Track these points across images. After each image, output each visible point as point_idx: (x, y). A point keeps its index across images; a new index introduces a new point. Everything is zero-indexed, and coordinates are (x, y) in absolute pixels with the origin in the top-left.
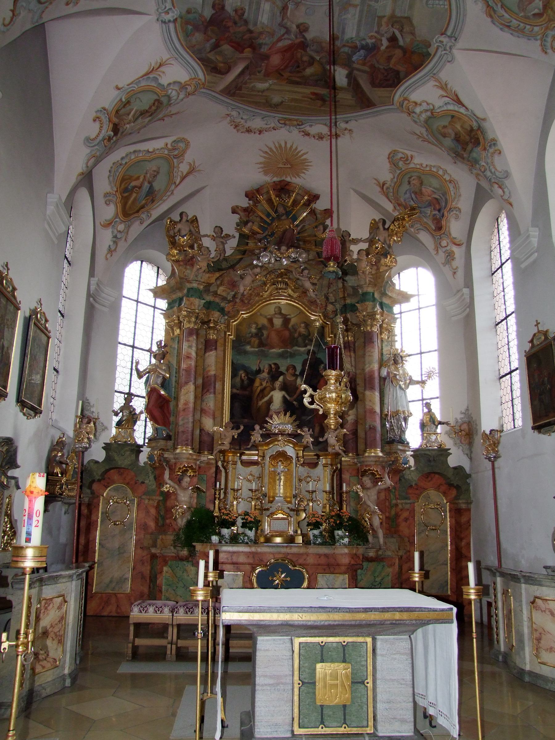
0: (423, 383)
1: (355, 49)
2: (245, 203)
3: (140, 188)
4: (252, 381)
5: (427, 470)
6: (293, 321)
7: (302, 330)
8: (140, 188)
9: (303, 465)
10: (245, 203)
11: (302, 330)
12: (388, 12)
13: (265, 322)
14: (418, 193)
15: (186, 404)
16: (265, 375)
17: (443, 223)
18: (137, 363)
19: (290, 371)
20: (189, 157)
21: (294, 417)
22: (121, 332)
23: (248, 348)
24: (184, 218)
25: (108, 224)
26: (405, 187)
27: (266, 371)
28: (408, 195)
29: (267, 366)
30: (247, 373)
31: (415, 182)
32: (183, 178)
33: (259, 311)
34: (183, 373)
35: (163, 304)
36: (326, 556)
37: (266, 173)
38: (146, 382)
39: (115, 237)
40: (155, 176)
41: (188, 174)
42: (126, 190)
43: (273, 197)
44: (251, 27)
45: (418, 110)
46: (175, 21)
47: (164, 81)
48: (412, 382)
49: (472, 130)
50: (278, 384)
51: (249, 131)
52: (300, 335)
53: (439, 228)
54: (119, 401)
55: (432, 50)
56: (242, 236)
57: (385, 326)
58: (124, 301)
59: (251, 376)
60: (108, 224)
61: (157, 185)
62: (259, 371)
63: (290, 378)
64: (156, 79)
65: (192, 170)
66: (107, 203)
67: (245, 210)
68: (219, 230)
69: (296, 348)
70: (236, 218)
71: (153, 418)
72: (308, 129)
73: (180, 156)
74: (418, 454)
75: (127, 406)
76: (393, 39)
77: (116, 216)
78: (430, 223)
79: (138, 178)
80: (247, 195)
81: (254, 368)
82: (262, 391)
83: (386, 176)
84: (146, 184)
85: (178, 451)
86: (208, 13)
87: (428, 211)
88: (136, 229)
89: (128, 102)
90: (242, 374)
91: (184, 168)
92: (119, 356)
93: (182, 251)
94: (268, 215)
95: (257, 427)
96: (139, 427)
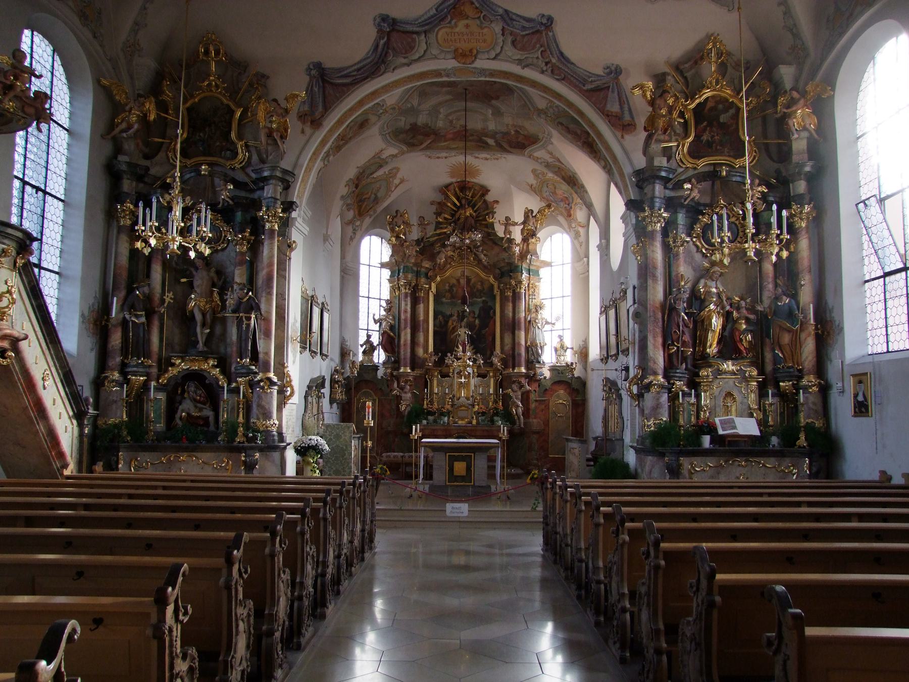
0: (554, 324)
1: (496, 133)
2: (440, 198)
3: (369, 198)
4: (447, 322)
5: (557, 379)
6: (473, 281)
7: (479, 287)
8: (369, 198)
9: (478, 377)
10: (440, 198)
11: (479, 287)
12: (511, 123)
13: (454, 281)
14: (554, 193)
15: (406, 341)
16: (455, 318)
17: (572, 212)
18: (374, 315)
19: (472, 315)
20: (399, 176)
21: (472, 347)
22: (361, 289)
23: (444, 300)
24: (399, 215)
25: (351, 222)
26: (545, 189)
27: (456, 315)
28: (548, 193)
29: (456, 312)
30: (443, 317)
31: (551, 186)
32: (396, 187)
33: (450, 274)
34: (402, 321)
35: (386, 273)
36: (487, 431)
37: (452, 177)
38: (380, 326)
39: (354, 230)
40: (378, 191)
41: (400, 183)
42: (360, 201)
43: (458, 192)
44: (433, 128)
45: (539, 161)
46: (389, 133)
47: (384, 156)
48: (547, 323)
49: (570, 177)
50: (463, 324)
51: (438, 158)
52: (478, 290)
53: (570, 215)
54: (362, 338)
55: (541, 137)
56: (438, 223)
57: (531, 286)
58: (361, 266)
59: (447, 318)
60: (351, 222)
61: (379, 195)
62: (451, 316)
63: (471, 320)
64: (379, 157)
65: (402, 181)
66: (348, 210)
67: (439, 203)
68: (422, 218)
69: (475, 299)
70: (434, 208)
71: (385, 350)
72: (477, 155)
73: (394, 176)
74: (553, 369)
75: (368, 341)
76: (517, 131)
77: (354, 217)
78: (563, 211)
79: (368, 193)
80: (440, 192)
81: (448, 313)
82: (453, 328)
83: (532, 180)
84: (373, 195)
85: (401, 371)
86: (408, 127)
87: (562, 204)
88: (368, 221)
89: (364, 172)
90: (440, 317)
91: (397, 181)
92: (361, 306)
93: (398, 237)
94: (455, 205)
95: (449, 354)
96: (376, 353)
